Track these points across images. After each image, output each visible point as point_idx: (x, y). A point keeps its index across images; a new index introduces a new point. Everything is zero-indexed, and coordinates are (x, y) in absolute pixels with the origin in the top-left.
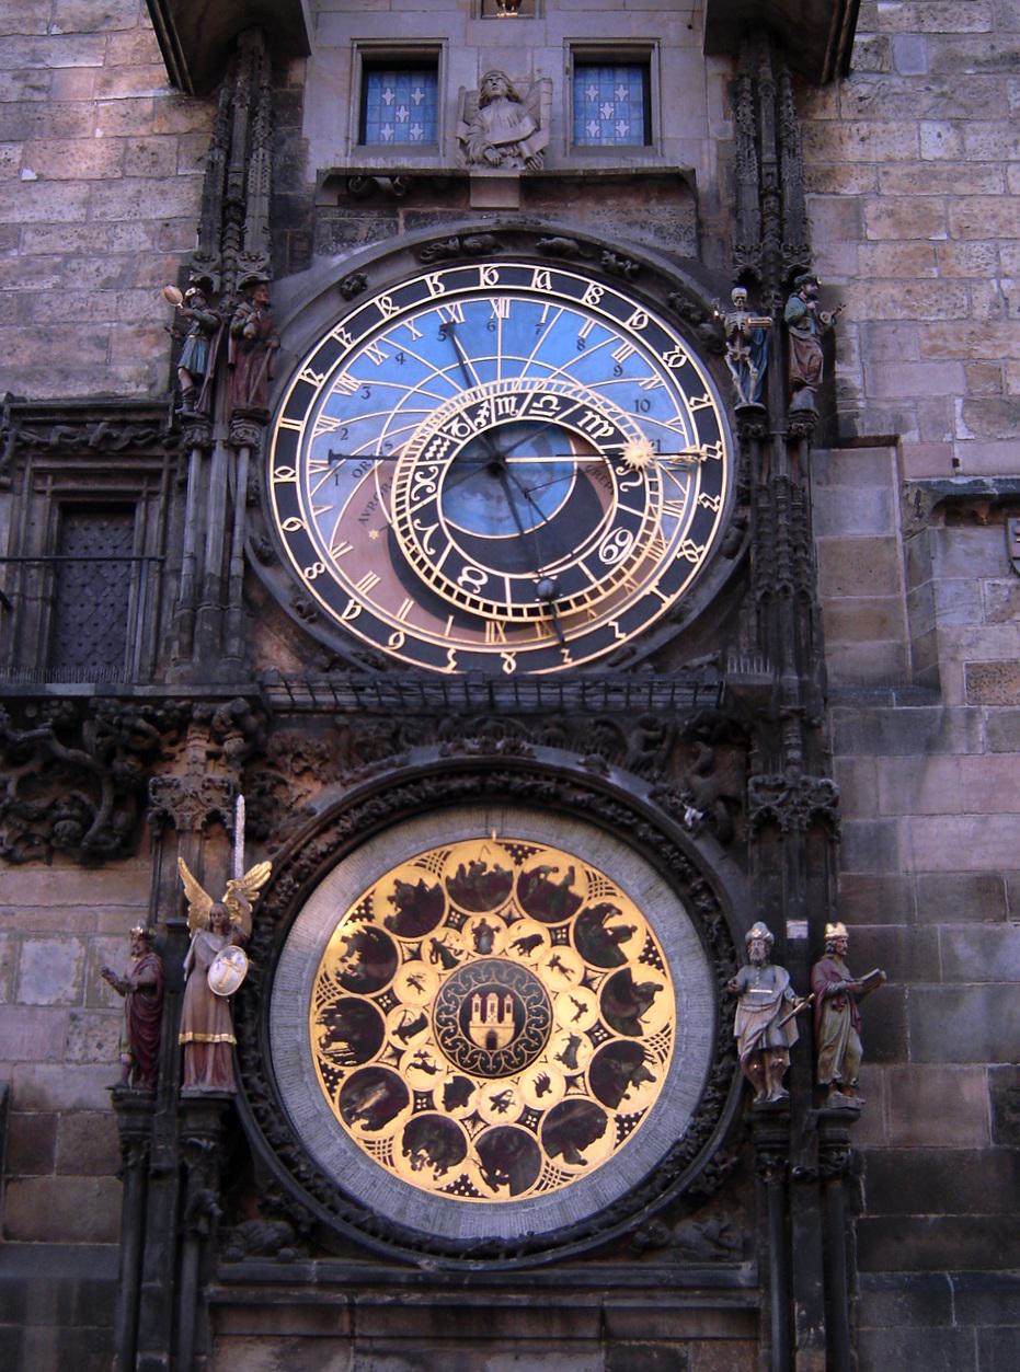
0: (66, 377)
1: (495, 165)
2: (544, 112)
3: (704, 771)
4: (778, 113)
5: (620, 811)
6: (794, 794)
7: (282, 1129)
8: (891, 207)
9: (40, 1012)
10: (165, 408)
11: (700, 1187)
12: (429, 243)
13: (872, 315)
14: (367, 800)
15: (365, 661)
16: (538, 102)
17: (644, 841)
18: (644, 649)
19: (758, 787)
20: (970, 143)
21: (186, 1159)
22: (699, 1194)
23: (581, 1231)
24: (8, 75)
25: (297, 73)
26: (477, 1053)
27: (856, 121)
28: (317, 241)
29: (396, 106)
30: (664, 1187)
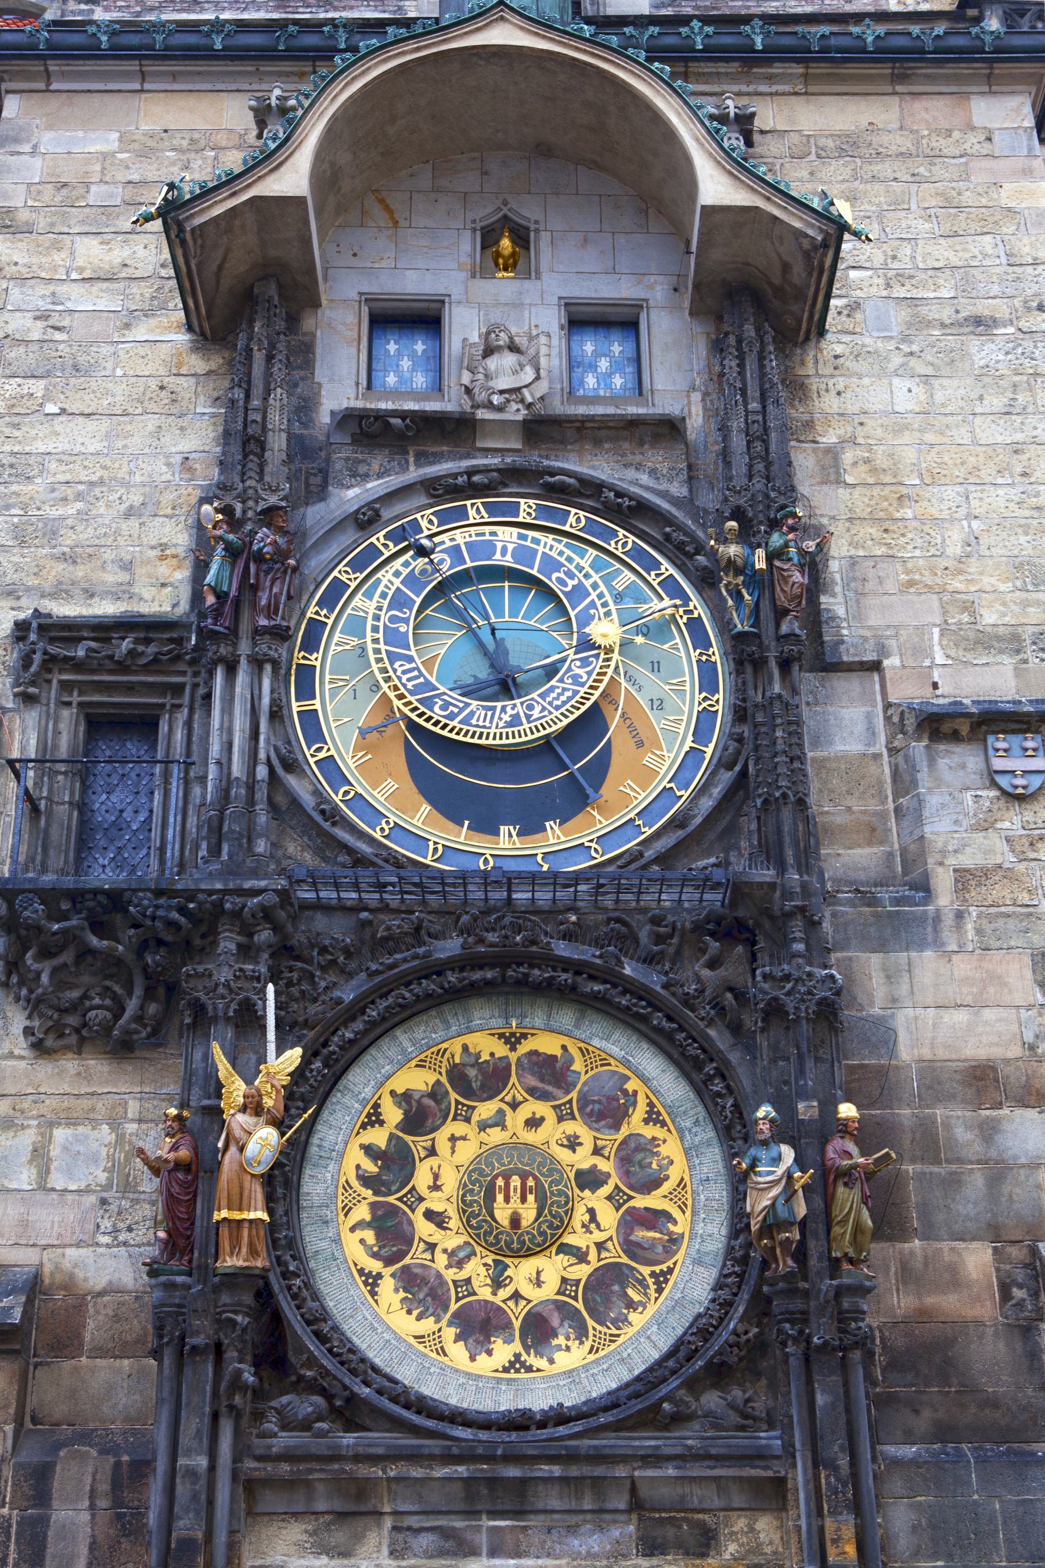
0: (92, 596)
1: (500, 409)
2: (543, 362)
3: (712, 965)
4: (762, 366)
5: (634, 1001)
6: (800, 983)
8: (867, 455)
9: (69, 1197)
10: (187, 627)
11: (724, 1358)
12: (439, 478)
13: (853, 552)
14: (392, 990)
15: (387, 861)
16: (538, 353)
17: (658, 1030)
18: (649, 854)
19: (765, 977)
20: (939, 397)
21: (222, 1336)
22: (723, 1364)
23: (611, 1402)
24: (30, 315)
25: (308, 323)
26: (502, 1233)
27: (832, 376)
28: (331, 475)
29: (399, 354)
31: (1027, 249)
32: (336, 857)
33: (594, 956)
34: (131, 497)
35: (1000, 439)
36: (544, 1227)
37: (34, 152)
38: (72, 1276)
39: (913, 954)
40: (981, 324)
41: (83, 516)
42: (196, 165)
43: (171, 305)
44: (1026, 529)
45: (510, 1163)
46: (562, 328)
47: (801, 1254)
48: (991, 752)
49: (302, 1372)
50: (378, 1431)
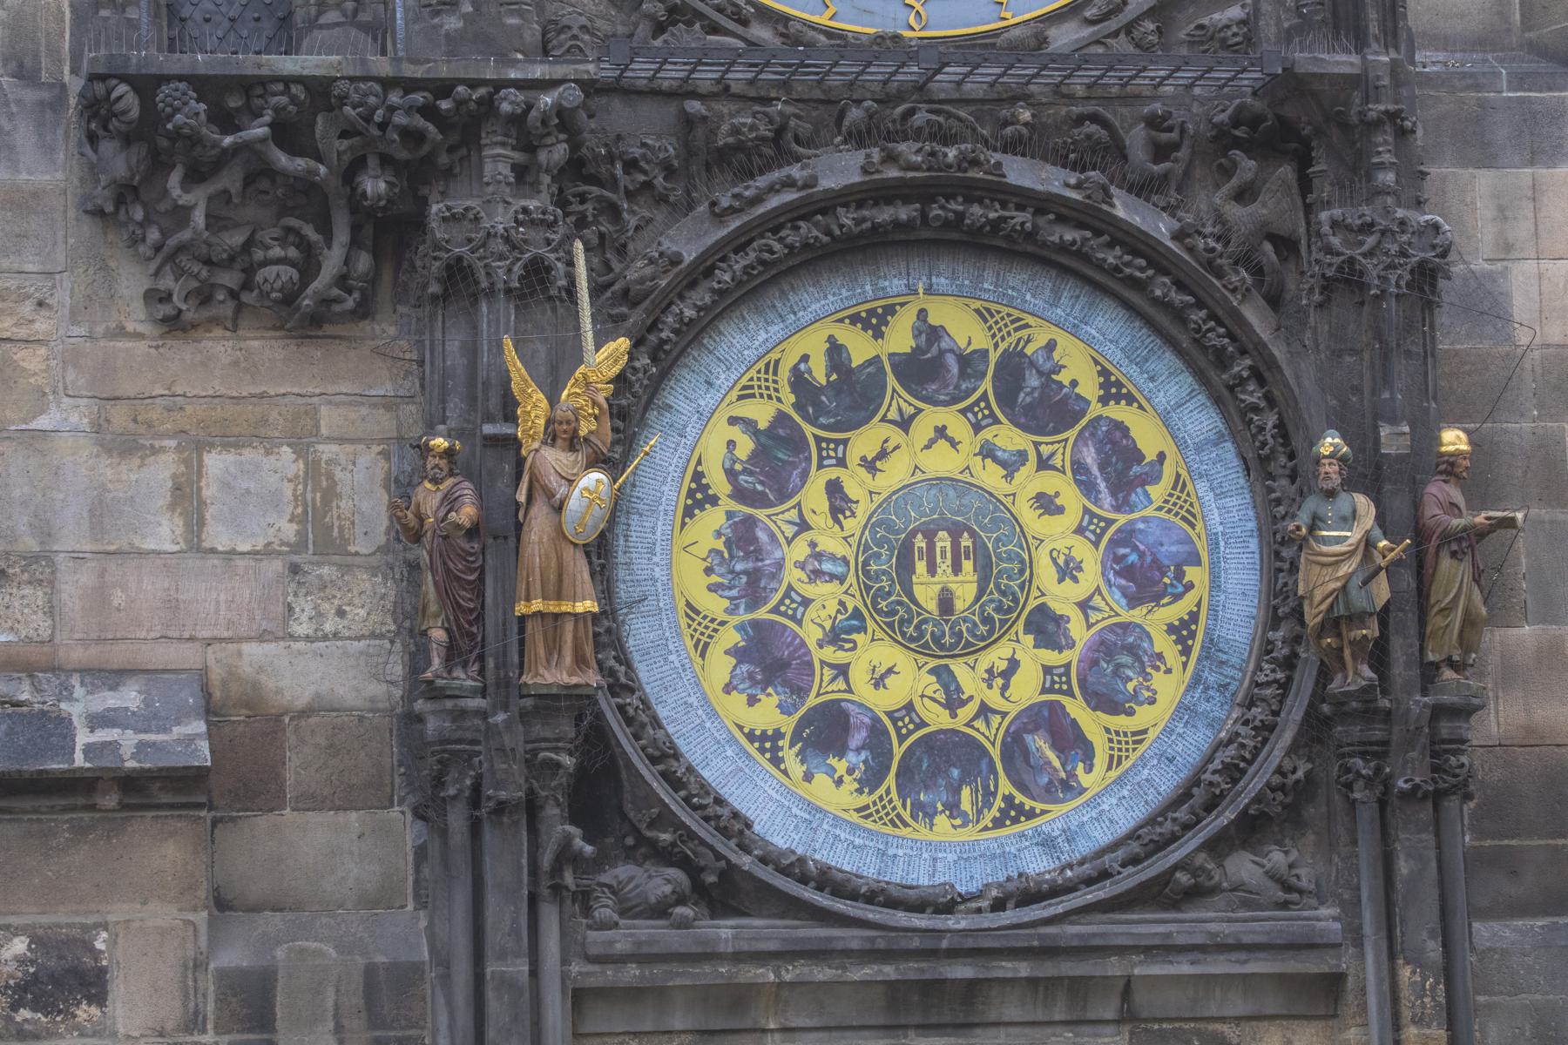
3: (1244, 195)
5: (1127, 258)
7: (660, 733)
9: (240, 563)
17: (1164, 305)
19: (1335, 224)
21: (536, 785)
30: (1211, 805)
33: (1067, 185)
36: (989, 609)
38: (256, 685)
45: (933, 511)
47: (1379, 656)
49: (649, 834)
50: (761, 916)
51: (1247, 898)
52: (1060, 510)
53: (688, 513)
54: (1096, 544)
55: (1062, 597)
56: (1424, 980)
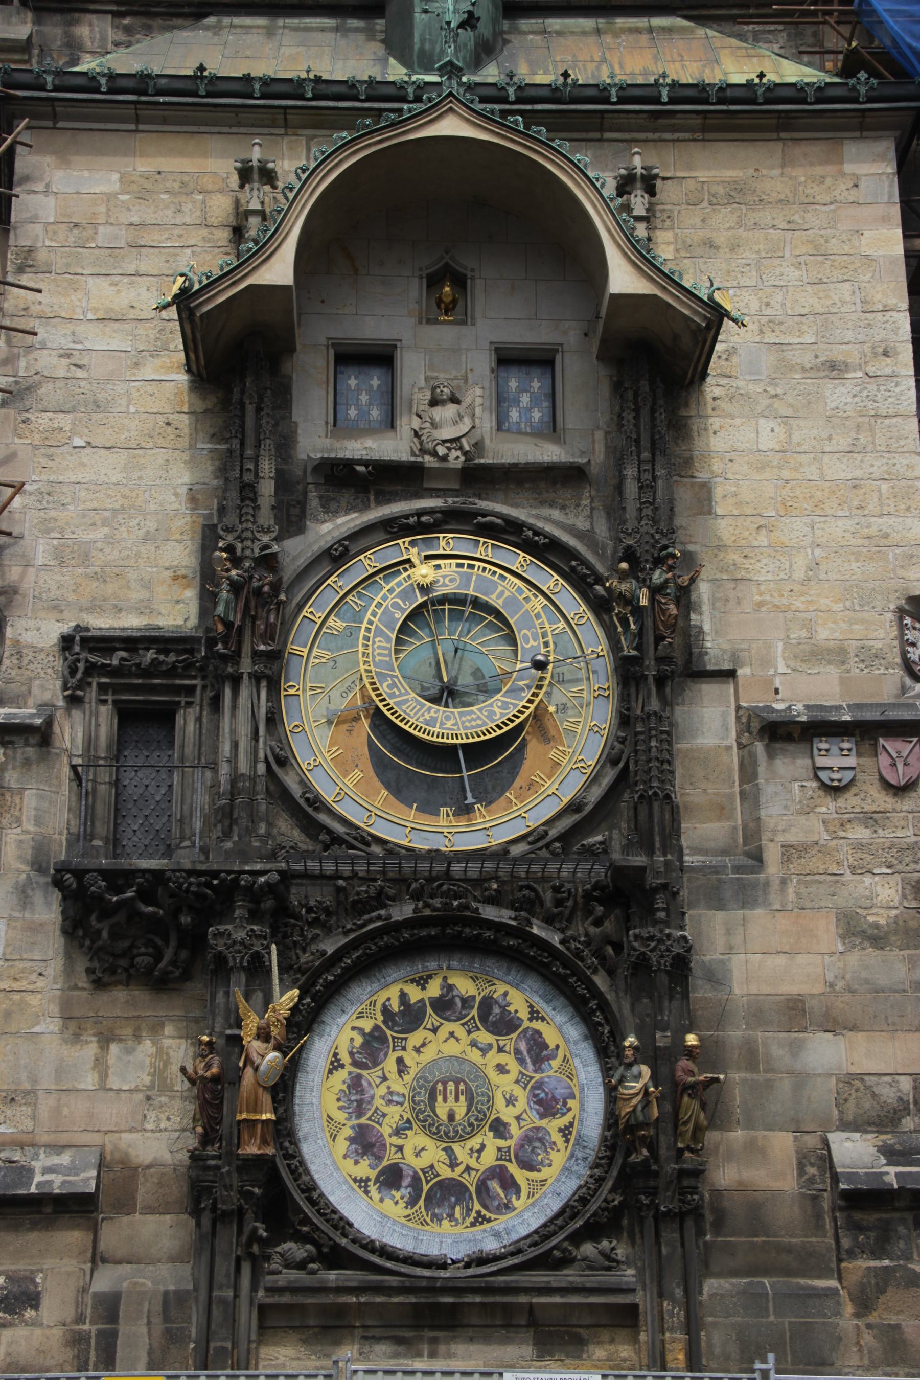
0: (120, 610)
3: (598, 923)
4: (653, 419)
8: (734, 489)
10: (197, 640)
15: (355, 839)
18: (553, 833)
19: (636, 937)
20: (796, 437)
24: (54, 353)
28: (308, 512)
29: (359, 390)
31: (878, 297)
32: (319, 835)
34: (148, 523)
35: (842, 475)
36: (472, 1120)
37: (46, 192)
38: (127, 1154)
39: (748, 912)
40: (835, 369)
41: (110, 540)
42: (187, 208)
43: (172, 347)
44: (857, 557)
46: (492, 371)
48: (815, 751)
51: (590, 1265)
52: (508, 1072)
53: (330, 1072)
54: (525, 1088)
55: (507, 1114)
56: (674, 1308)
